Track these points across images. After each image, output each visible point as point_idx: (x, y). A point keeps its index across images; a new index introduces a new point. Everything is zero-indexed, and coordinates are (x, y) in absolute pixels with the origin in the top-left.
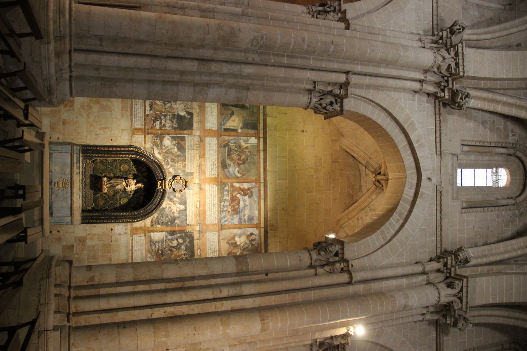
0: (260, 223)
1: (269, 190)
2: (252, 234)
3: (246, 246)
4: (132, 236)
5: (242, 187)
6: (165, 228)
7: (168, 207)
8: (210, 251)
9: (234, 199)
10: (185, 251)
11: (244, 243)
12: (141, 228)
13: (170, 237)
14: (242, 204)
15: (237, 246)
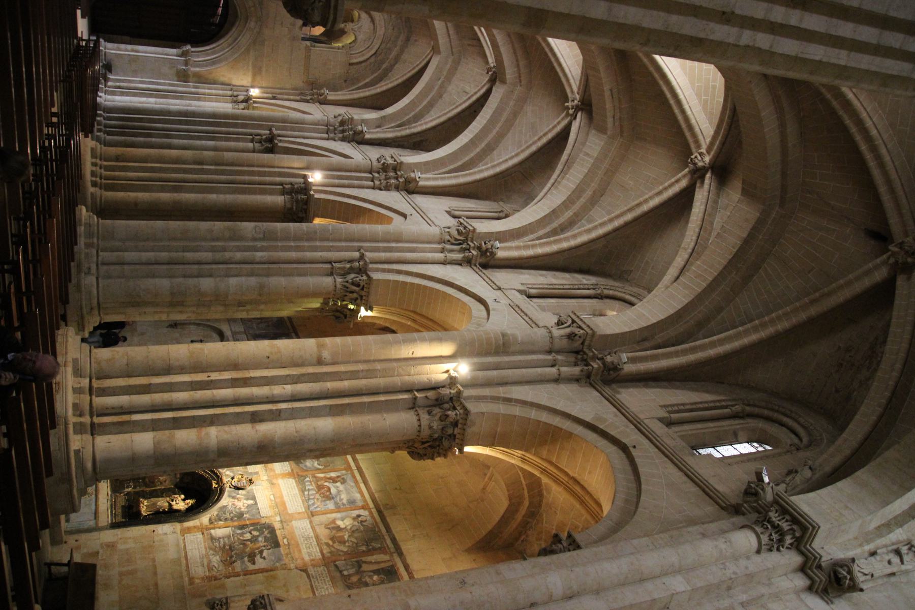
0: (368, 504)
1: (367, 476)
2: (359, 516)
3: (354, 528)
4: (184, 536)
5: (328, 476)
6: (229, 523)
7: (230, 504)
8: (302, 539)
9: (320, 488)
10: (265, 542)
11: (351, 526)
12: (195, 527)
13: (239, 532)
14: (333, 491)
15: (343, 529)
